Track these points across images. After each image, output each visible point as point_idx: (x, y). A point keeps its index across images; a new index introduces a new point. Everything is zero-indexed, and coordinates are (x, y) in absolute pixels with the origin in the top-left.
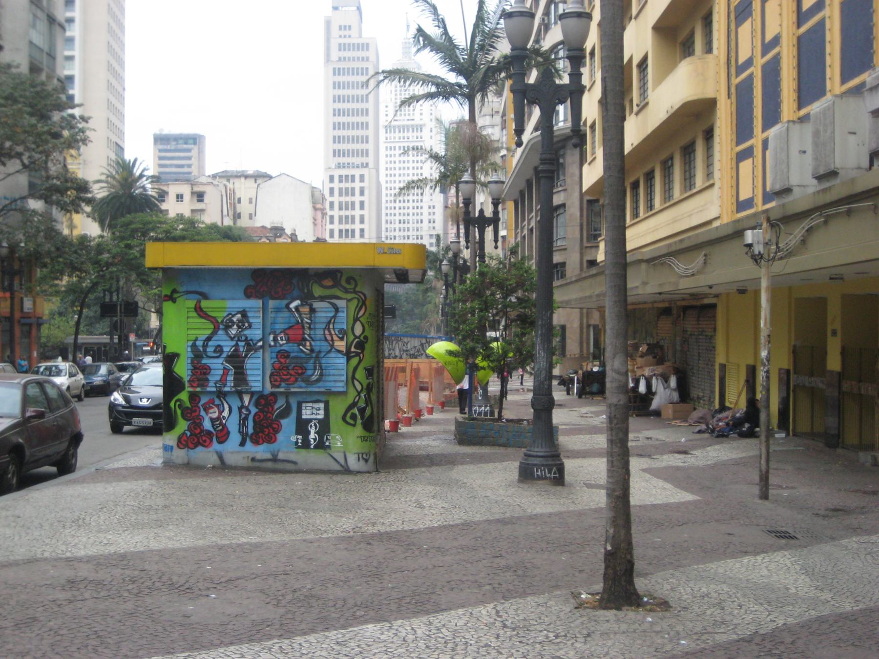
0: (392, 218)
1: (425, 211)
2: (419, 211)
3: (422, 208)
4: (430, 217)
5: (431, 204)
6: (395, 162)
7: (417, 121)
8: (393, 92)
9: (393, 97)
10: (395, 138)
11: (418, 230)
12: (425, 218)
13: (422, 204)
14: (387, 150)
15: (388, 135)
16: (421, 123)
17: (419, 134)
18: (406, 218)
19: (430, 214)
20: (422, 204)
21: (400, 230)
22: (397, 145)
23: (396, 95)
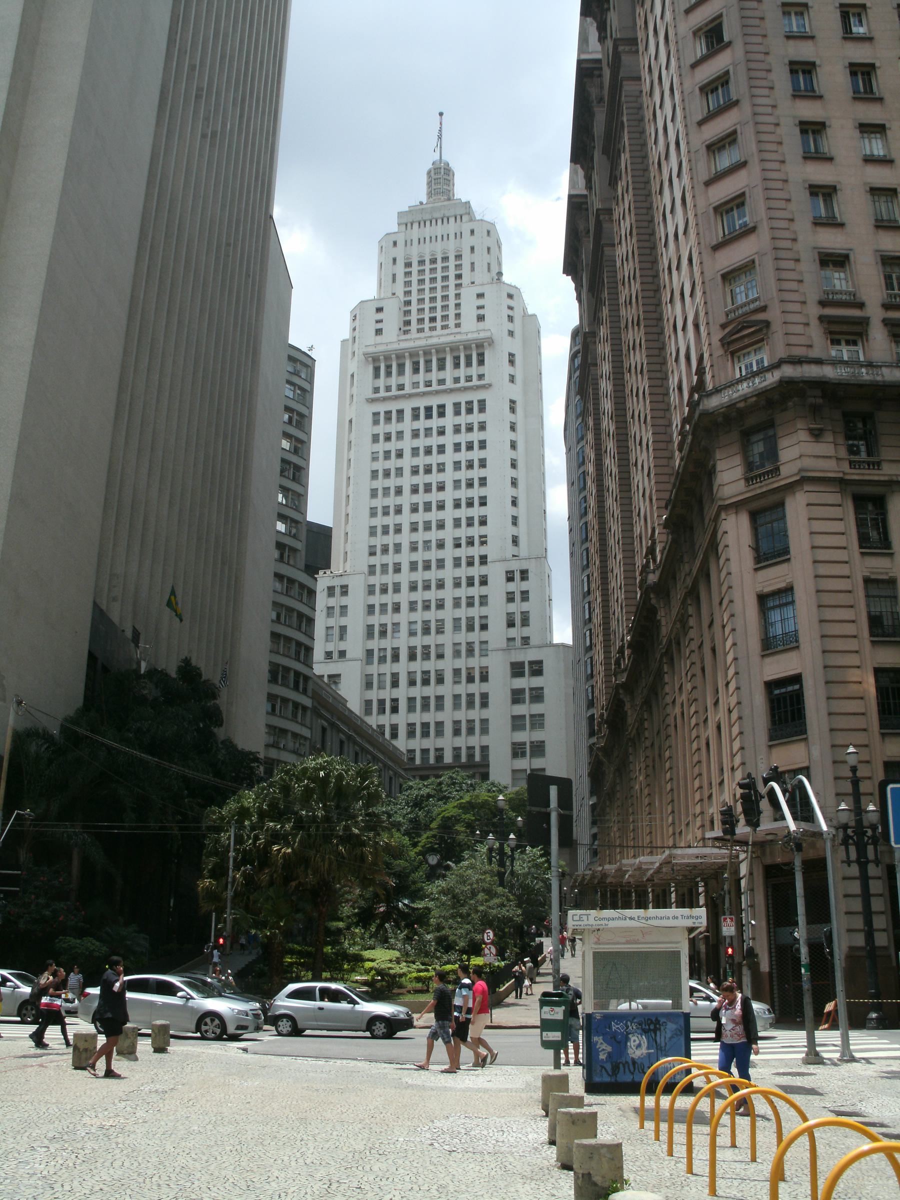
0: (388, 619)
1: (497, 588)
2: (476, 591)
3: (484, 582)
4: (512, 607)
5: (515, 566)
6: (400, 455)
7: (470, 329)
8: (401, 278)
9: (400, 289)
10: (401, 387)
11: (470, 652)
12: (497, 610)
13: (484, 570)
14: (376, 422)
15: (381, 382)
16: (482, 335)
17: (474, 371)
18: (432, 615)
19: (510, 598)
20: (484, 570)
21: (412, 657)
22: (407, 407)
23: (408, 284)
